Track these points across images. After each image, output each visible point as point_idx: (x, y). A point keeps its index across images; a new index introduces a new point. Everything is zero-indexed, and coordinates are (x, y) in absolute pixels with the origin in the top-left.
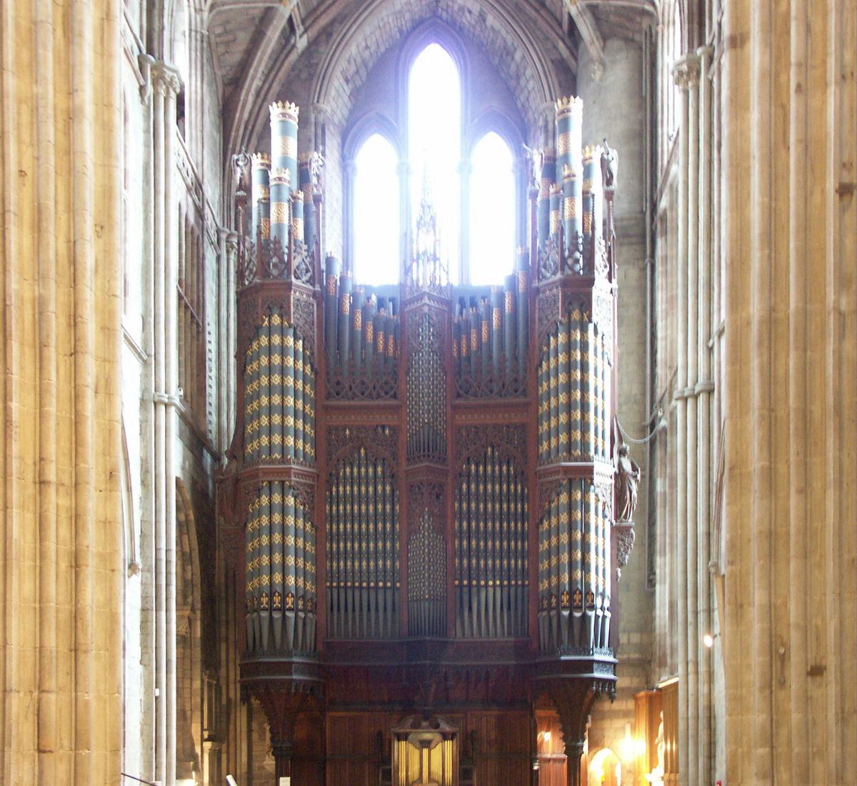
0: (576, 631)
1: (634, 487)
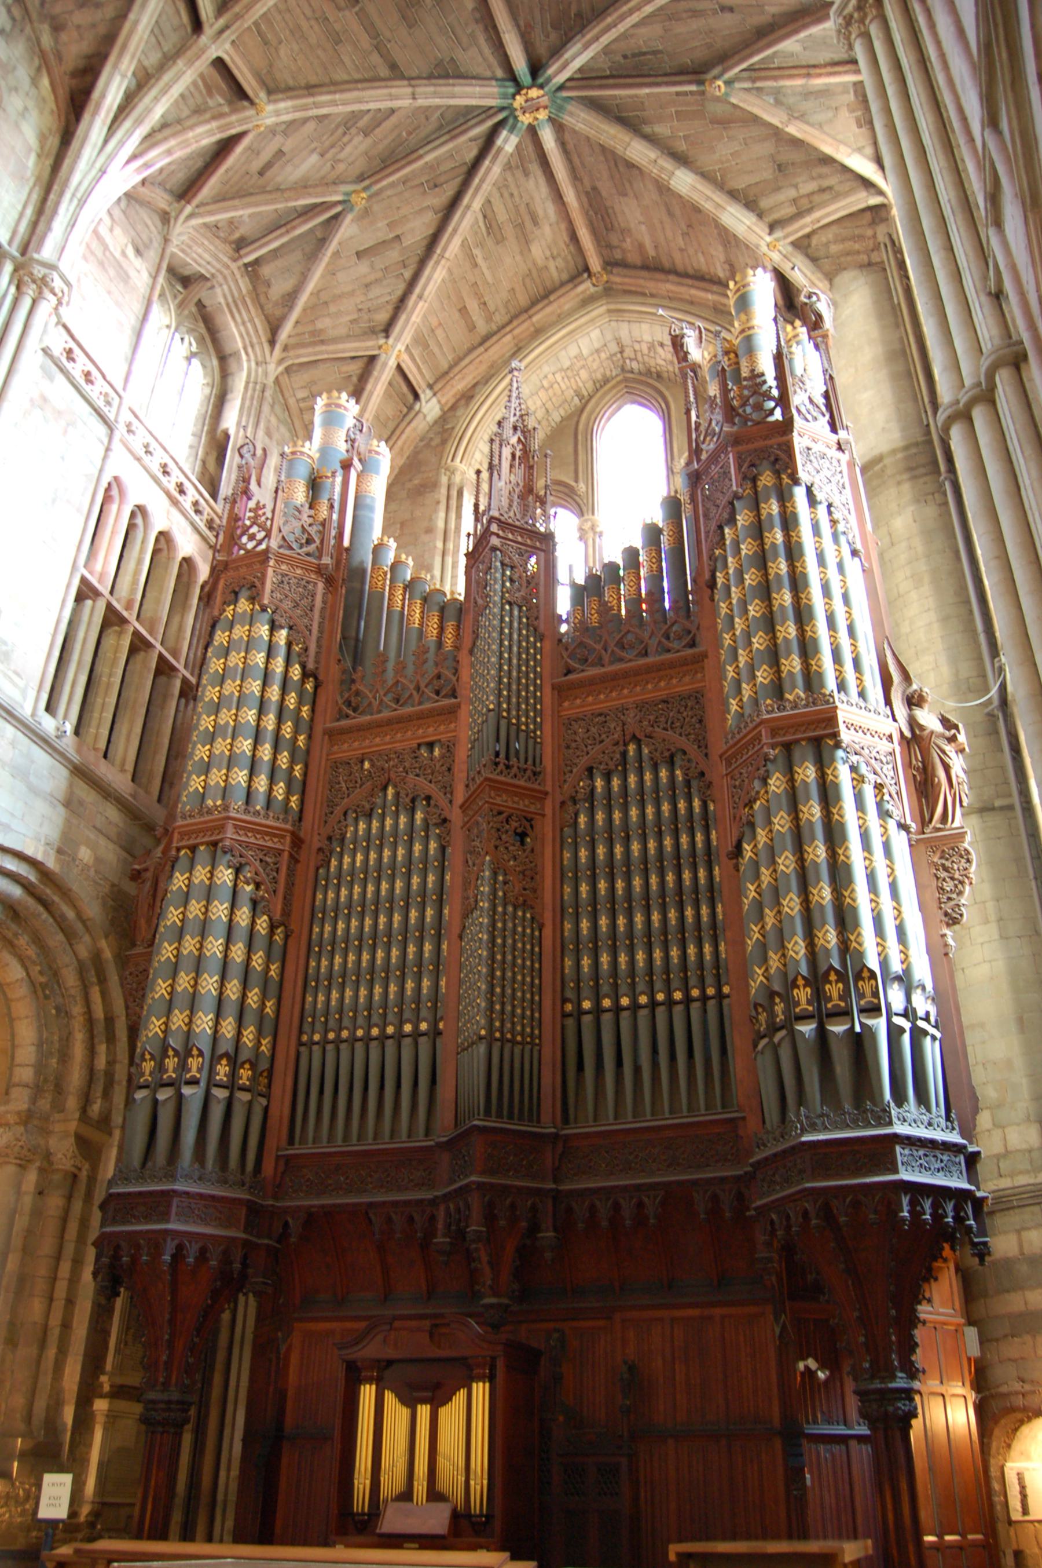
0: (842, 1068)
1: (958, 765)
